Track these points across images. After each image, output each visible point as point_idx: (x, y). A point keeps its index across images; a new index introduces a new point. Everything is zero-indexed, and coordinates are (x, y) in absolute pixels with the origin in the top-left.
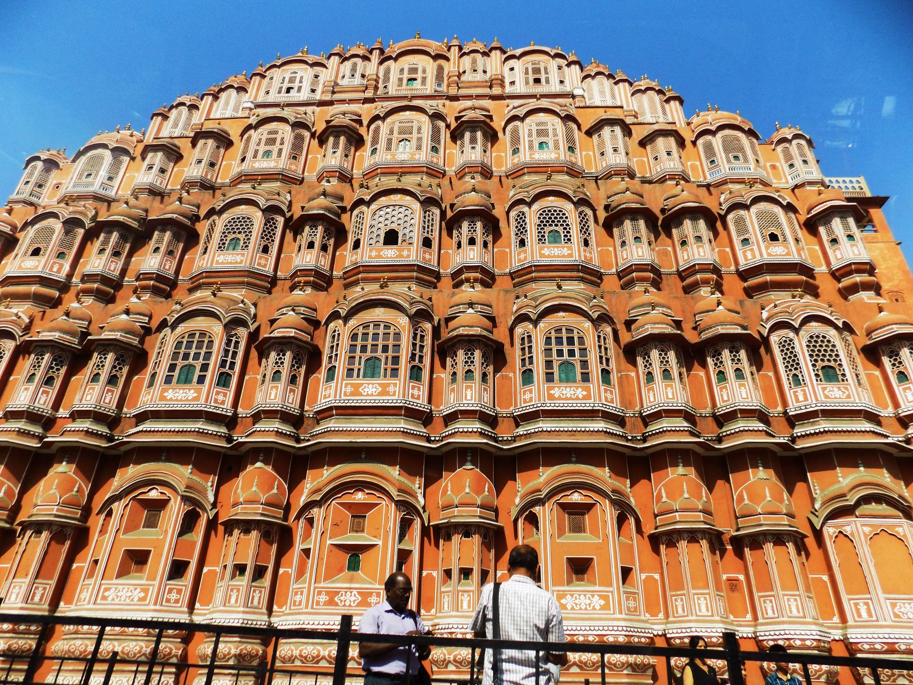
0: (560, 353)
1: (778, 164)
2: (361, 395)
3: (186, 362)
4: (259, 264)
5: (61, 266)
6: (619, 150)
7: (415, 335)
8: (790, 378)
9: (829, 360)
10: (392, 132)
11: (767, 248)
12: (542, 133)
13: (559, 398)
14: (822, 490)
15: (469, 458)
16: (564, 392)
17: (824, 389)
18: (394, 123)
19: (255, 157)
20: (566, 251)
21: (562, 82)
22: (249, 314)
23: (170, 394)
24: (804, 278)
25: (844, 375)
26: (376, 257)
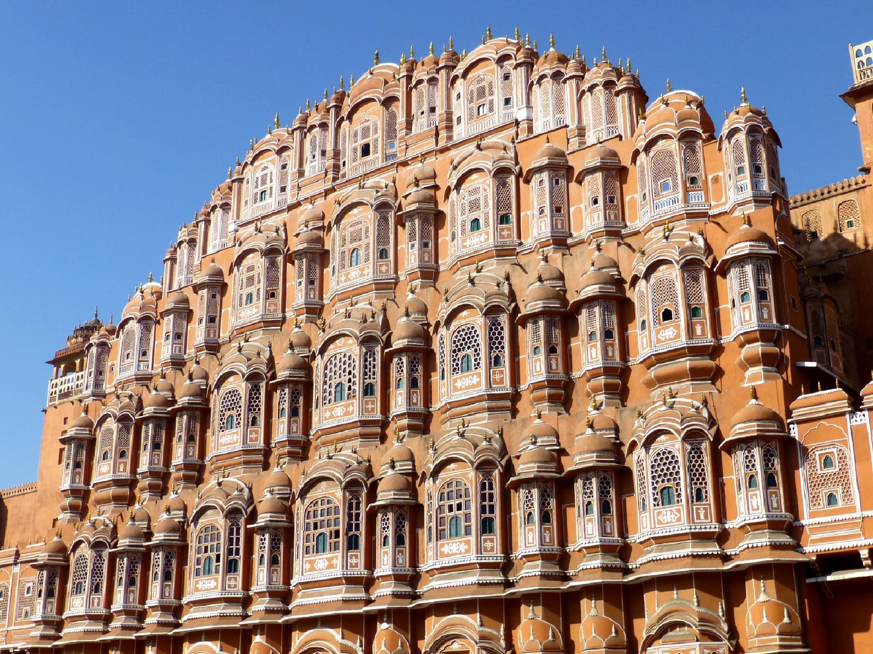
0: (451, 508)
1: (721, 174)
2: (315, 570)
3: (206, 555)
4: (251, 440)
5: (125, 463)
7: (351, 504)
9: (669, 480)
12: (474, 205)
13: (448, 555)
19: (241, 305)
20: (475, 380)
21: (507, 101)
22: (242, 499)
23: (200, 586)
25: (679, 495)
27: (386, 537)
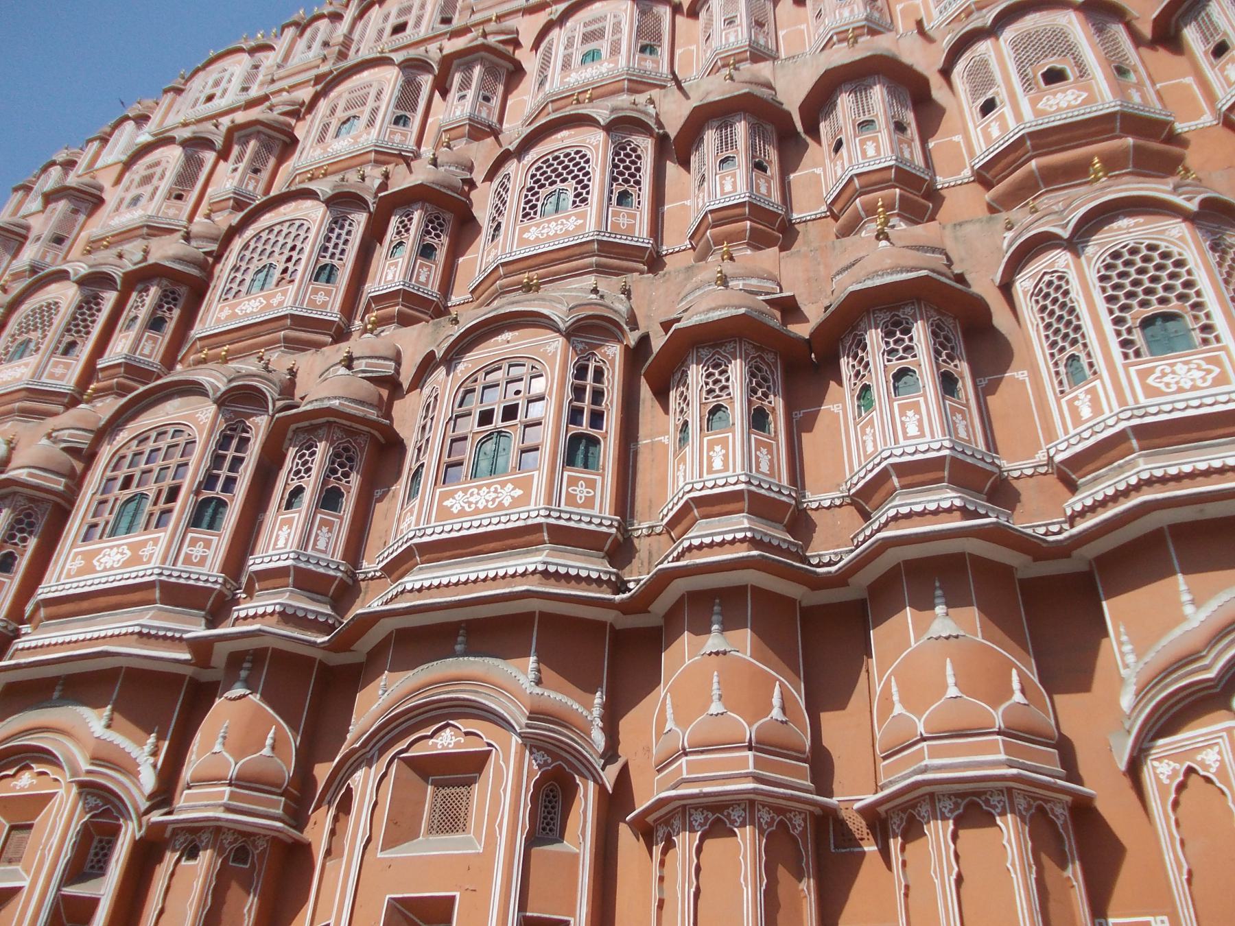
4: (52, 376)
6: (738, 21)
8: (1062, 369)
9: (1163, 301)
10: (333, 111)
11: (1034, 102)
13: (463, 512)
14: (1139, 653)
15: (243, 674)
16: (473, 499)
17: (1143, 375)
18: (340, 96)
19: (117, 209)
20: (571, 224)
24: (1130, 141)
25: (1207, 328)
26: (227, 318)
27: (299, 490)
